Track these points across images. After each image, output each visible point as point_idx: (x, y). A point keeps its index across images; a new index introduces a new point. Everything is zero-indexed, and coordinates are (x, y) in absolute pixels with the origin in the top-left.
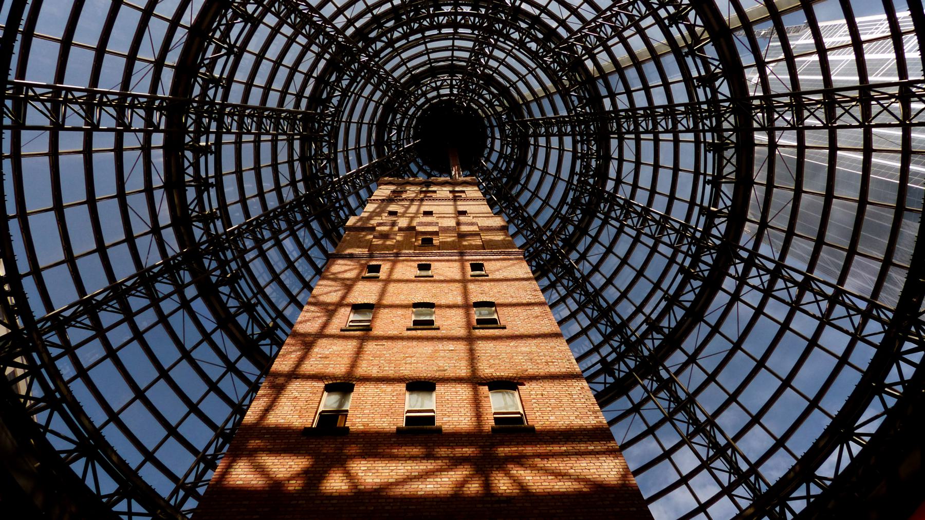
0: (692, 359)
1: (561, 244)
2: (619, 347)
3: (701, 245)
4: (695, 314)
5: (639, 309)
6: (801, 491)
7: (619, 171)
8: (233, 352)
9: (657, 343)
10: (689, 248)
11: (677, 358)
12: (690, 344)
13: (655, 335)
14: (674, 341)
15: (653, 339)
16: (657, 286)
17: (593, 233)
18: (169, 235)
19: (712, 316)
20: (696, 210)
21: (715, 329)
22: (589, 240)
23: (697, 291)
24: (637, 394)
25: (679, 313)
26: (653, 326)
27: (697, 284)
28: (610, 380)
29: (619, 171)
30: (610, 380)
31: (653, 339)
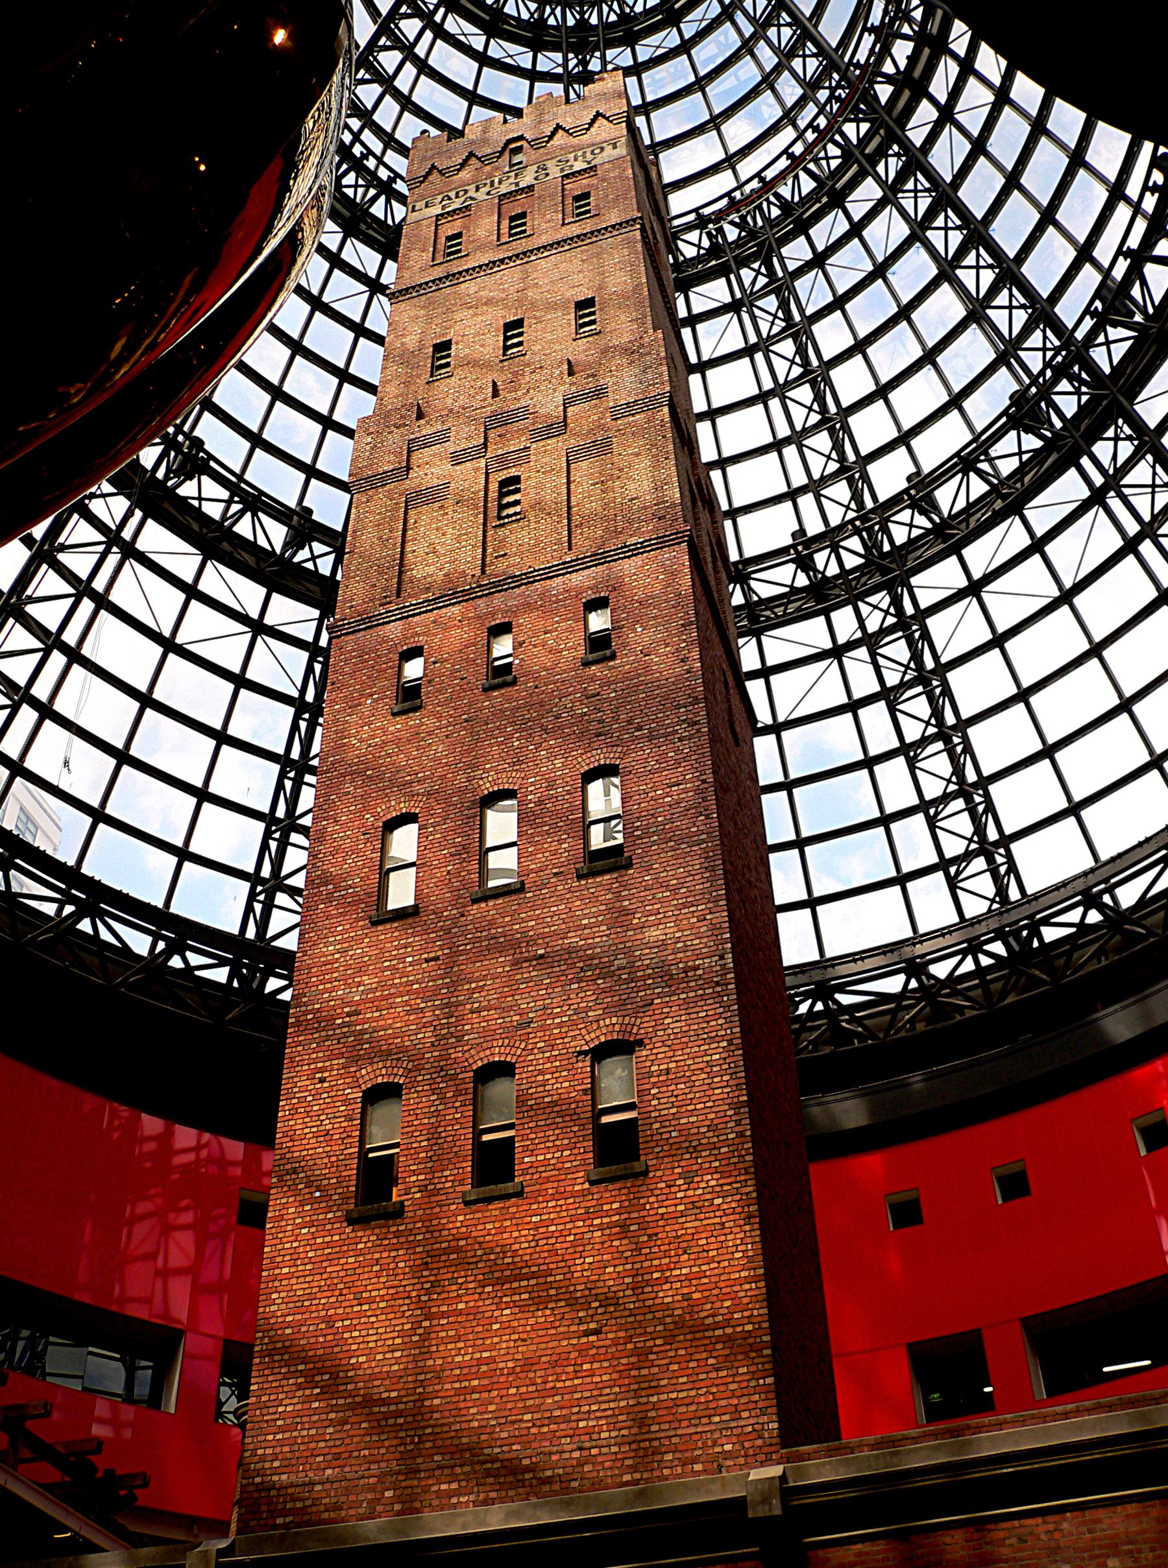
0: (974, 588)
1: (775, 212)
3: (1073, 356)
4: (1010, 499)
5: (904, 439)
6: (1074, 916)
7: (955, 93)
9: (916, 532)
10: (1042, 373)
11: (943, 577)
12: (982, 554)
14: (950, 536)
17: (858, 211)
20: (1088, 280)
21: (1038, 546)
22: (843, 227)
23: (1025, 457)
24: (845, 622)
25: (978, 488)
27: (1032, 442)
28: (802, 581)
29: (955, 93)
30: (802, 581)
31: (911, 526)
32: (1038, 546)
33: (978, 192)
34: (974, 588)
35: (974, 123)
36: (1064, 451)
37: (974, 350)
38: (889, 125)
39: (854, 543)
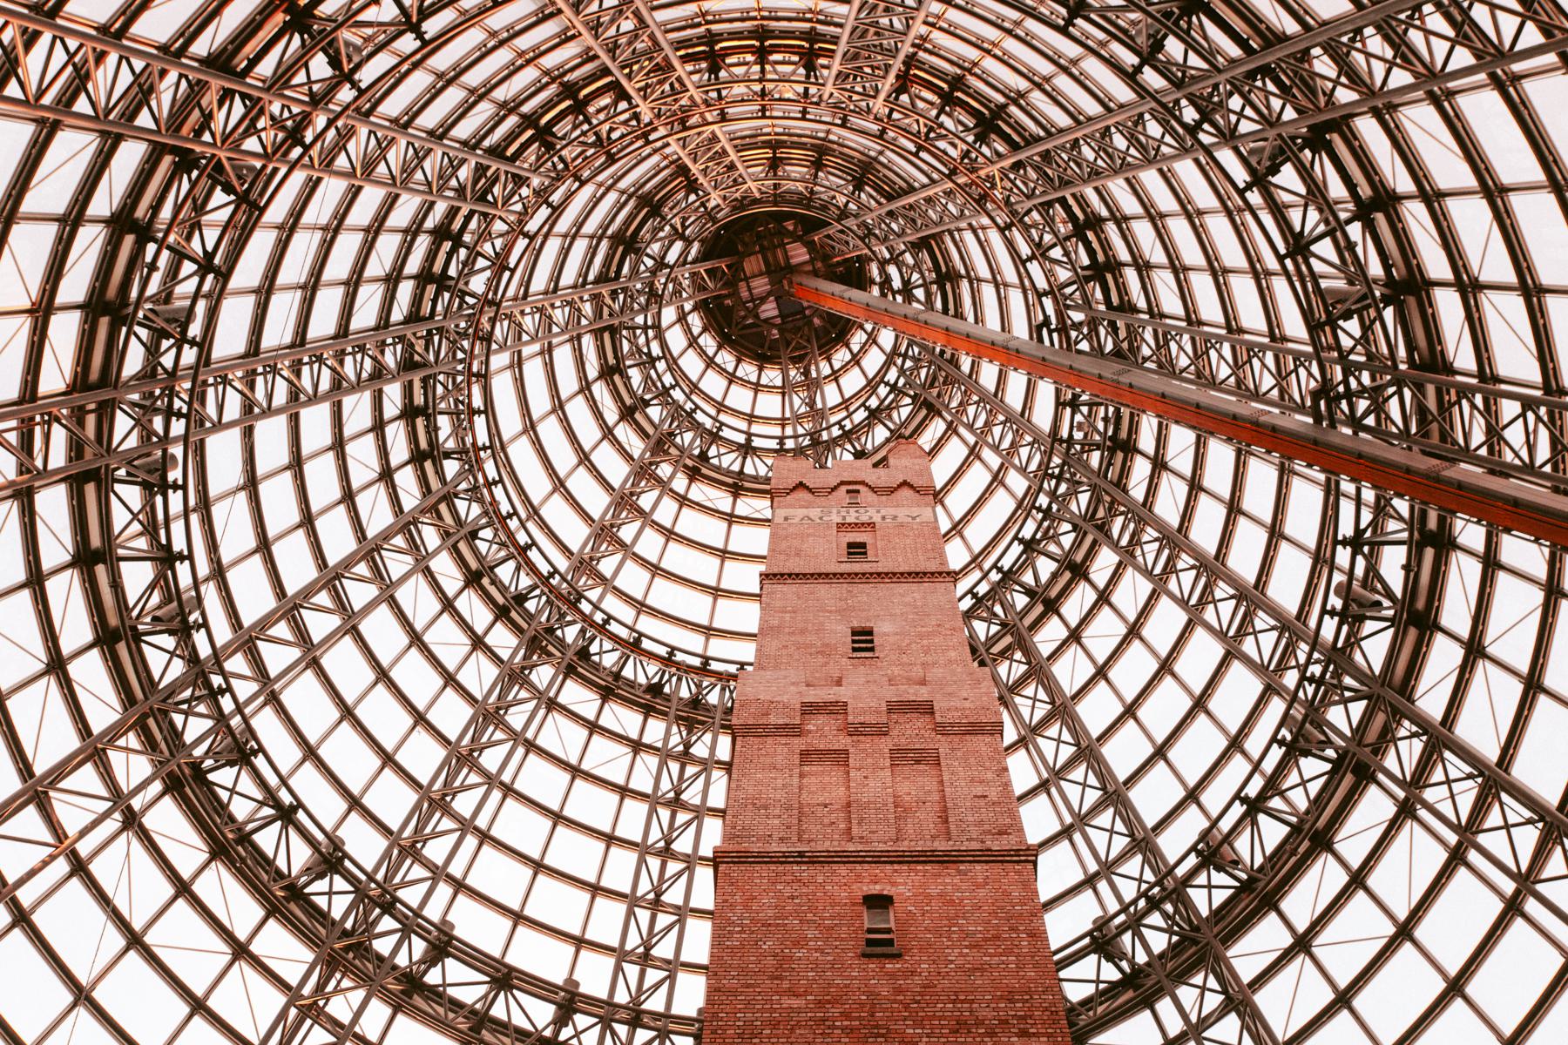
0: (1302, 944)
2: (1135, 902)
4: (1313, 836)
8: (242, 911)
9: (1220, 897)
11: (1267, 937)
12: (1301, 903)
13: (1219, 878)
14: (1261, 893)
15: (1210, 887)
16: (1236, 744)
18: (90, 673)
19: (1354, 841)
21: (1358, 879)
26: (1212, 852)
30: (1110, 973)
31: (1210, 887)
32: (1358, 879)
33: (1206, 531)
34: (1302, 944)
35: (1184, 464)
36: (1356, 768)
37: (1241, 688)
38: (1109, 490)
39: (1155, 919)
